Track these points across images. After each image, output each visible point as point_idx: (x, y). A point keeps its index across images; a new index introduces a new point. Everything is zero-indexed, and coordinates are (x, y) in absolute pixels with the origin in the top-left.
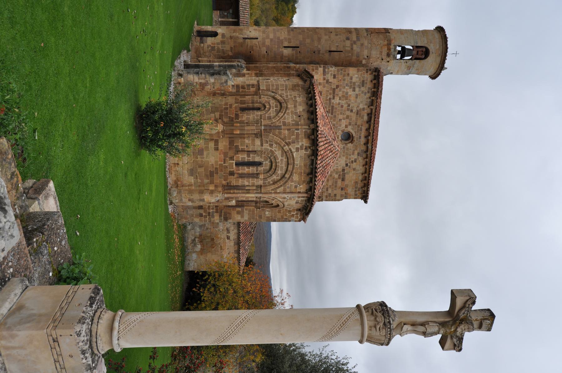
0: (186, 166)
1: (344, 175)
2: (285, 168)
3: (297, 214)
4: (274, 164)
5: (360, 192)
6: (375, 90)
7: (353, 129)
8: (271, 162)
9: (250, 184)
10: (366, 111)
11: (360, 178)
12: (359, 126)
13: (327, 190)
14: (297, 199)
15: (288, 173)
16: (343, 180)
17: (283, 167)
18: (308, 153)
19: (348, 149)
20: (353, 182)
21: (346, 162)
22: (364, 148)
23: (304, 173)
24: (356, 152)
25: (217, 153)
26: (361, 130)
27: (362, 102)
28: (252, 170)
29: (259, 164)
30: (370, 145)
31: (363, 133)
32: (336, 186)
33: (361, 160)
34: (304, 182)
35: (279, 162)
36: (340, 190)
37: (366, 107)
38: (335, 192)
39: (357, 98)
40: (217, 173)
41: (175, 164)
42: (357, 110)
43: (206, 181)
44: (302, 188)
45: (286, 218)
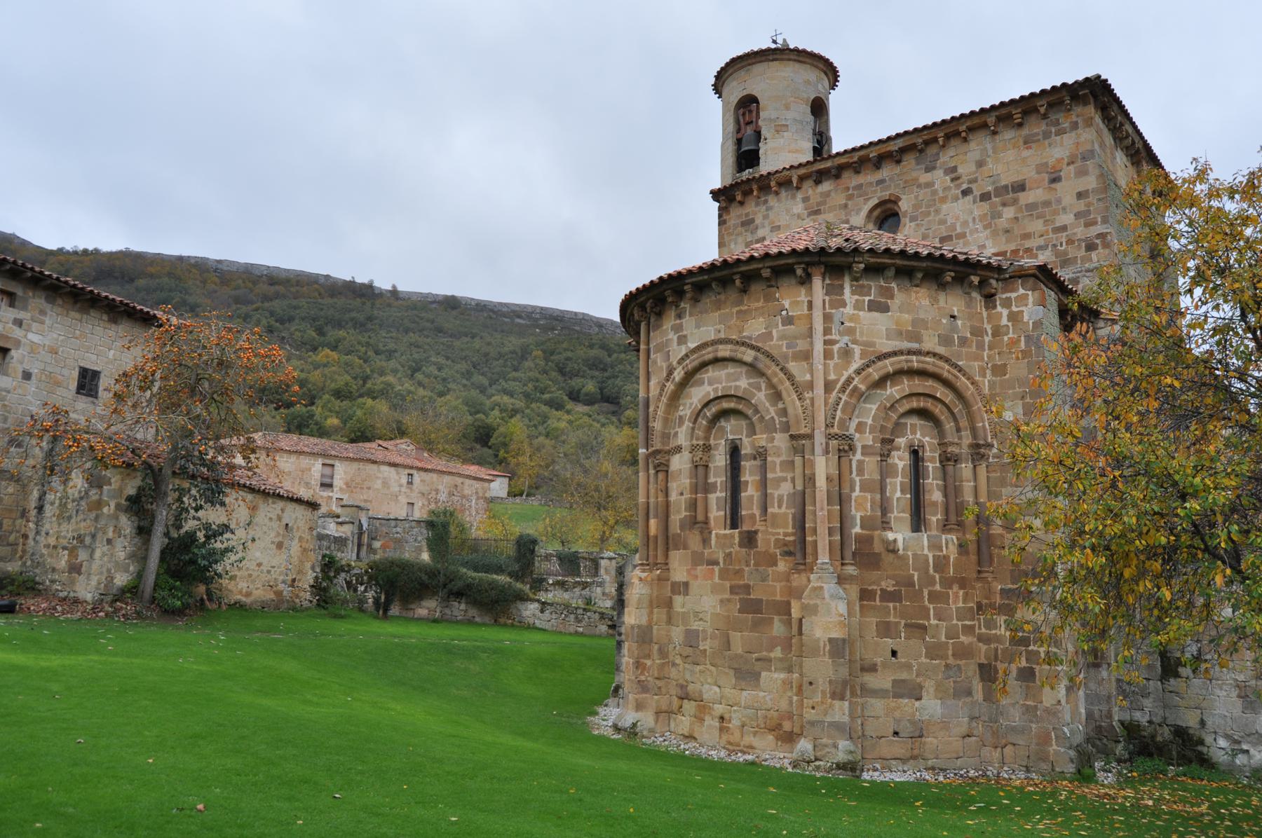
0: (728, 691)
1: (1001, 190)
2: (731, 369)
3: (1007, 303)
4: (726, 405)
5: (1061, 116)
6: (755, 187)
7: (859, 210)
8: (725, 413)
9: (789, 476)
10: (810, 192)
11: (1008, 134)
12: (850, 197)
13: (1064, 228)
14: (849, 310)
15: (739, 356)
16: (1020, 187)
17: (728, 375)
18: (688, 306)
19: (916, 207)
20: (1026, 153)
21: (956, 199)
22: (909, 160)
23: (740, 303)
24: (925, 178)
25: (695, 586)
26: (860, 187)
27: (788, 211)
28: (749, 476)
29: (734, 452)
30: (894, 147)
31: (868, 177)
32: (1047, 204)
33: (948, 157)
34: (769, 298)
35: (716, 390)
36: (1057, 185)
37: (800, 196)
38: (1069, 199)
39: (778, 228)
40: (747, 588)
41: (721, 729)
42: (809, 215)
43: (778, 628)
44: (791, 299)
45: (1028, 338)
